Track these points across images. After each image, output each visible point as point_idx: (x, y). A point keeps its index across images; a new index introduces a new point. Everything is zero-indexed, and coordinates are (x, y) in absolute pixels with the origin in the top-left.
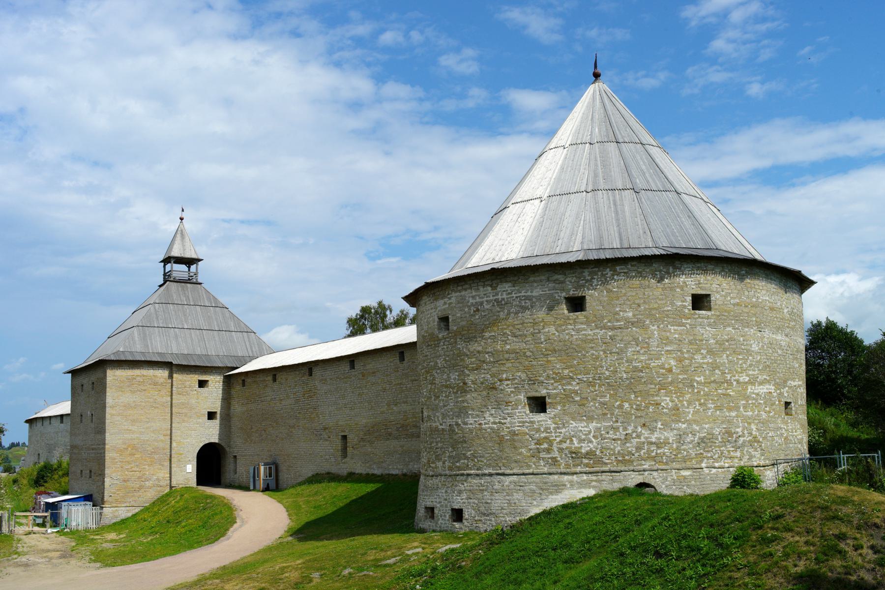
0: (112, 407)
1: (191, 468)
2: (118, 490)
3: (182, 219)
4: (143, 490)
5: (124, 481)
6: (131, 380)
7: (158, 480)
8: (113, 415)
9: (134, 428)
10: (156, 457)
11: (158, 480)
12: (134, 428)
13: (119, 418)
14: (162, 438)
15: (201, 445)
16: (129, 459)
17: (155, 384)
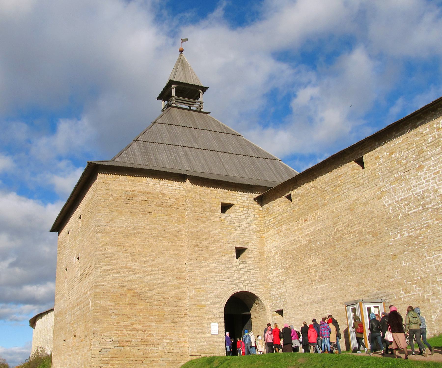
0: (105, 233)
1: (217, 328)
2: (113, 358)
3: (181, 51)
4: (147, 361)
5: (122, 344)
6: (131, 196)
7: (170, 344)
8: (104, 244)
9: (135, 266)
10: (167, 309)
11: (170, 344)
12: (135, 266)
13: (115, 249)
14: (174, 281)
15: (230, 294)
16: (127, 311)
17: (164, 205)
